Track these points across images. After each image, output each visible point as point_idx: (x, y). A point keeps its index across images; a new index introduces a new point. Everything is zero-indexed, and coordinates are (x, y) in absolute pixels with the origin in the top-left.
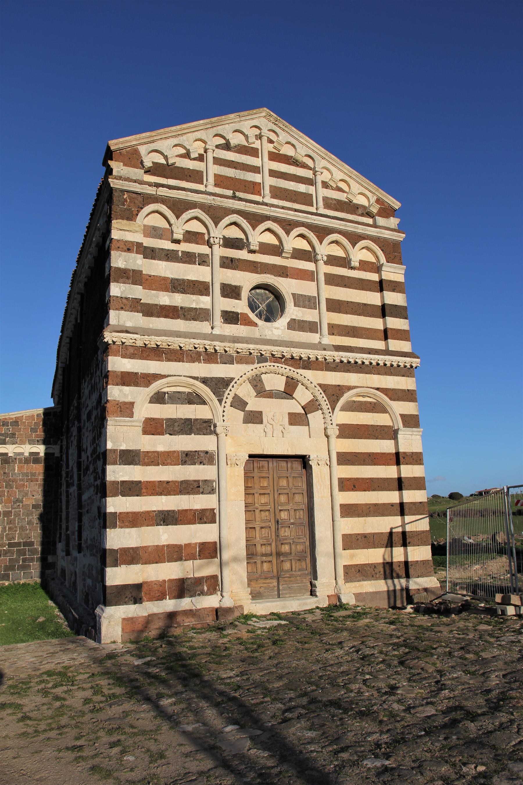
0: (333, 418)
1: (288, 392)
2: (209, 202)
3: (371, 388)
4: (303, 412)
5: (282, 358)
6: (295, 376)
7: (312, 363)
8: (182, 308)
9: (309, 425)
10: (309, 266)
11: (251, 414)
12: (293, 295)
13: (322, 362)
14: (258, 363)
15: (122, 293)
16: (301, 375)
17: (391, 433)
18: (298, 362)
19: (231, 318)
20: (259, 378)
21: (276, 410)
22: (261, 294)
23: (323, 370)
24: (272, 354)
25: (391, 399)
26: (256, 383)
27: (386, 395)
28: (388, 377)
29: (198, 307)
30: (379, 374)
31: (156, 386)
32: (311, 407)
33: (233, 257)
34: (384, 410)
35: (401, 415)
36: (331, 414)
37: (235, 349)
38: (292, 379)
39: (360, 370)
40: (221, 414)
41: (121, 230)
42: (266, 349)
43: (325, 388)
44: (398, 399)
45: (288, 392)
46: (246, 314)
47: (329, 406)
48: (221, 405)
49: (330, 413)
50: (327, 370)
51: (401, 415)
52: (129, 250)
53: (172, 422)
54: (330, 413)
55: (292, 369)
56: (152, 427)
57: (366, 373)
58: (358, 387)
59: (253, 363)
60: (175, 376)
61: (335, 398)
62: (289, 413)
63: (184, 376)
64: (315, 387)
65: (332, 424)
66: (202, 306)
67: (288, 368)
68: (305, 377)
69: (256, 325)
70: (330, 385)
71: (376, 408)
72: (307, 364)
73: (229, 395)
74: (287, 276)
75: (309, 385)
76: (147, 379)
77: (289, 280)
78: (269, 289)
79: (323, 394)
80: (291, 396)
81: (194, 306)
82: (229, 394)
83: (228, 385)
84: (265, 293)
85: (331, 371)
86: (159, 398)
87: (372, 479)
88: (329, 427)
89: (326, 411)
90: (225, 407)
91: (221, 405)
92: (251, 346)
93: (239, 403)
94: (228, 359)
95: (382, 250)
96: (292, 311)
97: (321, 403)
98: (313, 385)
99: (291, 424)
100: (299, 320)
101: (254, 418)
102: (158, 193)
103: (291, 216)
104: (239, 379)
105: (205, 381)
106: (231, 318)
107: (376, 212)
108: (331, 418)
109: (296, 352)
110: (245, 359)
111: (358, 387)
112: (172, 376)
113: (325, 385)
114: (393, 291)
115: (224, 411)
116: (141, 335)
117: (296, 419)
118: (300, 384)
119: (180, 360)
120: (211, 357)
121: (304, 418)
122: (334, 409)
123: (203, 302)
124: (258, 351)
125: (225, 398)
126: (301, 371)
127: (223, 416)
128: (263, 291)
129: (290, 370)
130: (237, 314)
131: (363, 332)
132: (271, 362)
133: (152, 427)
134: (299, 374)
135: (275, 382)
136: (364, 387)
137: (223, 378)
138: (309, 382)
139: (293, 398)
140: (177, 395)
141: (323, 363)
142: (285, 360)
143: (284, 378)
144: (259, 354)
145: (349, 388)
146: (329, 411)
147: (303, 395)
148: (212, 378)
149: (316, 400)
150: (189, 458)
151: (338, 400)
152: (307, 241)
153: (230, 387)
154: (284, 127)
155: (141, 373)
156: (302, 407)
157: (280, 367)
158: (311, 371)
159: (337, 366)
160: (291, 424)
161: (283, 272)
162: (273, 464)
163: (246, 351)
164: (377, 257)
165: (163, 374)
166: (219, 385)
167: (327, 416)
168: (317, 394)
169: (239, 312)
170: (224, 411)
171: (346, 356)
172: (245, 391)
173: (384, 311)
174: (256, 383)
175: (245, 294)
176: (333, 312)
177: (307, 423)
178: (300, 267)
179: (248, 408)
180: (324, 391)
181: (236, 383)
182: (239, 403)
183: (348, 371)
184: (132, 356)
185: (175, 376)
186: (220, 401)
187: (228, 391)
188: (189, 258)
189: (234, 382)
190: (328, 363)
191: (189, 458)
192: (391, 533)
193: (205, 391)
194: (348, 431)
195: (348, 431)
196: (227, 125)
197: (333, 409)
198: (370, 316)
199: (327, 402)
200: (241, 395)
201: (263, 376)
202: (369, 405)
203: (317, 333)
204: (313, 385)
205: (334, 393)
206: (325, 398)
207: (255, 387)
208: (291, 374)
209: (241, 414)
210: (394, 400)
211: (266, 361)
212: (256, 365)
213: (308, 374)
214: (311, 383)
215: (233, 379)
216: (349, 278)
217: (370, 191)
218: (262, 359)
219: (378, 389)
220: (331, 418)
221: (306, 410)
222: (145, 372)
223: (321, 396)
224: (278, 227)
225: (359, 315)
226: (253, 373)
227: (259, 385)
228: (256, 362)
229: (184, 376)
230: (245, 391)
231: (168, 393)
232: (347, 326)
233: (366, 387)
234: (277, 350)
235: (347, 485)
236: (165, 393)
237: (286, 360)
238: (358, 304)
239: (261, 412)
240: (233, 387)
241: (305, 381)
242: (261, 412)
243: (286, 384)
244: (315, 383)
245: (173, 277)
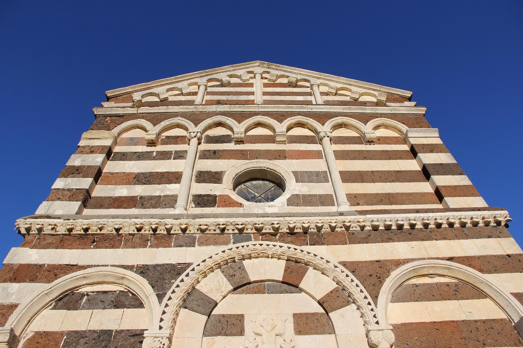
0: (379, 311)
1: (291, 283)
2: (191, 111)
3: (438, 258)
4: (323, 311)
5: (274, 235)
6: (299, 255)
7: (324, 236)
8: (141, 198)
9: (334, 332)
11: (223, 320)
12: (293, 172)
13: (342, 233)
14: (234, 243)
15: (65, 185)
16: (309, 253)
18: (303, 238)
20: (239, 266)
22: (260, 186)
23: (346, 244)
24: (257, 229)
25: (481, 271)
27: (470, 266)
28: (462, 241)
29: (162, 195)
30: (445, 239)
33: (216, 149)
34: (478, 293)
36: (373, 306)
37: (197, 227)
38: (297, 262)
39: (410, 236)
40: (159, 316)
41: (90, 139)
43: (353, 267)
45: (291, 283)
46: (228, 196)
47: (366, 293)
48: (160, 302)
49: (369, 304)
50: (352, 242)
52: (92, 152)
54: (369, 304)
55: (293, 246)
57: (423, 240)
58: (413, 260)
60: (98, 266)
61: (374, 280)
62: (295, 315)
63: (112, 266)
64: (336, 267)
65: (377, 323)
66: (168, 193)
67: (285, 246)
68: (315, 255)
70: (362, 262)
73: (179, 288)
74: (285, 158)
75: (325, 266)
77: (287, 161)
78: (268, 178)
79: (351, 276)
80: (297, 287)
82: (178, 286)
83: (179, 274)
84: (265, 184)
85: (359, 243)
86: (68, 301)
88: (372, 326)
89: (363, 303)
90: (167, 305)
91: (160, 302)
93: (195, 301)
95: (403, 123)
97: (351, 290)
98: (331, 265)
99: (299, 332)
100: (304, 196)
102: (139, 112)
103: (283, 108)
104: (199, 265)
107: (385, 100)
108: (373, 313)
111: (413, 260)
112: (95, 266)
113: (352, 263)
115: (164, 313)
116: (65, 220)
118: (311, 269)
121: (324, 321)
122: (377, 297)
123: (170, 190)
124: (234, 228)
125: (171, 290)
126: (307, 248)
127: (162, 320)
128: (261, 182)
129: (289, 248)
130: (215, 196)
131: (404, 198)
132: (256, 239)
134: (305, 252)
136: (424, 259)
137: (173, 265)
138: (324, 261)
139: (301, 290)
140: (102, 297)
141: (344, 234)
142: (281, 236)
144: (236, 231)
145: (398, 263)
146: (367, 301)
148: (156, 266)
149: (343, 289)
151: (381, 283)
152: (309, 129)
153: (183, 276)
154: (277, 68)
155: (49, 265)
156: (319, 302)
157: (271, 246)
158: (325, 246)
159: (370, 236)
160: (299, 332)
163: (214, 228)
164: (400, 131)
165: (81, 263)
167: (367, 309)
168: (342, 277)
169: (217, 194)
170: (164, 313)
171: (381, 220)
172: (216, 285)
173: (426, 173)
176: (352, 182)
177: (332, 331)
178: (301, 149)
180: (353, 272)
181: (193, 270)
182: (195, 301)
185: (98, 266)
186: (160, 297)
187: (177, 282)
188: (164, 156)
189: (191, 268)
190: (353, 234)
193: (142, 287)
196: (222, 73)
197: (375, 298)
198: (410, 181)
199: (362, 287)
201: (246, 263)
202: (446, 289)
203: (334, 205)
204: (331, 265)
206: (356, 281)
207: (230, 277)
208: (291, 253)
209: (200, 320)
211: (249, 239)
213: (321, 251)
214: (328, 262)
215: (189, 265)
216: (368, 151)
217: (374, 90)
219: (450, 259)
220: (373, 313)
221: (324, 305)
222: (54, 263)
223: (349, 279)
224: (269, 118)
225: (393, 181)
226: (225, 256)
227: (238, 274)
228: (232, 241)
229: (112, 266)
230: (216, 285)
231: (88, 295)
232: (377, 194)
233: (428, 259)
236: (83, 295)
237: (283, 235)
238: (389, 172)
239: (242, 316)
240: (187, 275)
241: (316, 261)
242: (242, 316)
243: (285, 270)
244: (334, 261)
245: (138, 172)
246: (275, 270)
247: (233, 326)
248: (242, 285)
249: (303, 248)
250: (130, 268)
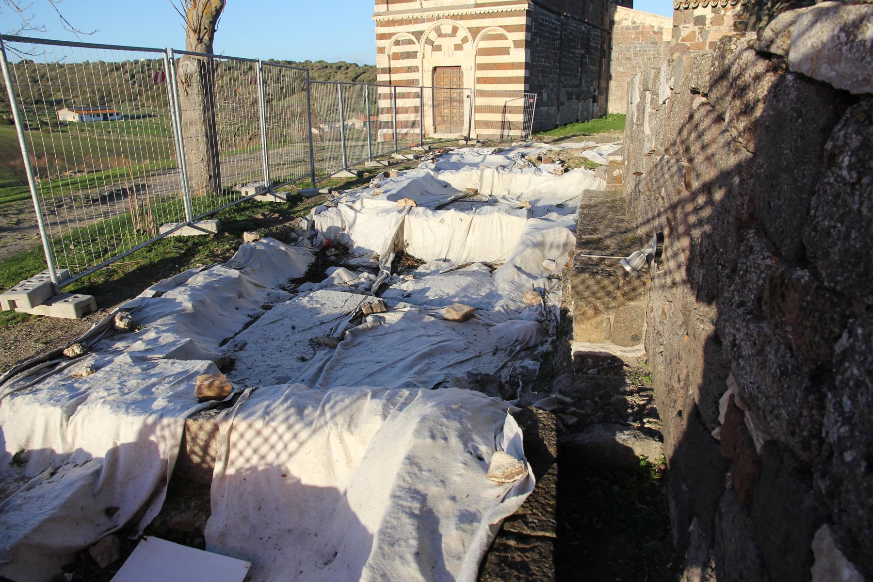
17: (505, 51)
21: (447, 43)
26: (438, 31)
31: (394, 38)
32: (465, 40)
34: (506, 38)
35: (514, 41)
42: (441, 13)
43: (470, 29)
44: (513, 31)
51: (514, 41)
53: (402, 53)
56: (396, 56)
71: (502, 37)
72: (462, 17)
73: (423, 38)
86: (397, 43)
87: (496, 78)
92: (431, 13)
94: (423, 21)
101: (438, 48)
105: (413, 33)
109: (456, 12)
117: (458, 47)
119: (402, 24)
120: (416, 21)
133: (396, 56)
135: (447, 28)
143: (451, 27)
145: (484, 28)
150: (410, 69)
162: (446, 69)
166: (418, 34)
172: (433, 36)
174: (438, 31)
182: (429, 42)
183: (483, 18)
184: (384, 26)
191: (410, 69)
192: (505, 106)
193: (413, 38)
194: (482, 52)
195: (482, 52)
205: (474, 32)
207: (437, 33)
218: (438, 18)
230: (433, 36)
234: (446, 13)
235: (480, 80)
246: (450, 31)
247: (438, 48)
248: (440, 35)
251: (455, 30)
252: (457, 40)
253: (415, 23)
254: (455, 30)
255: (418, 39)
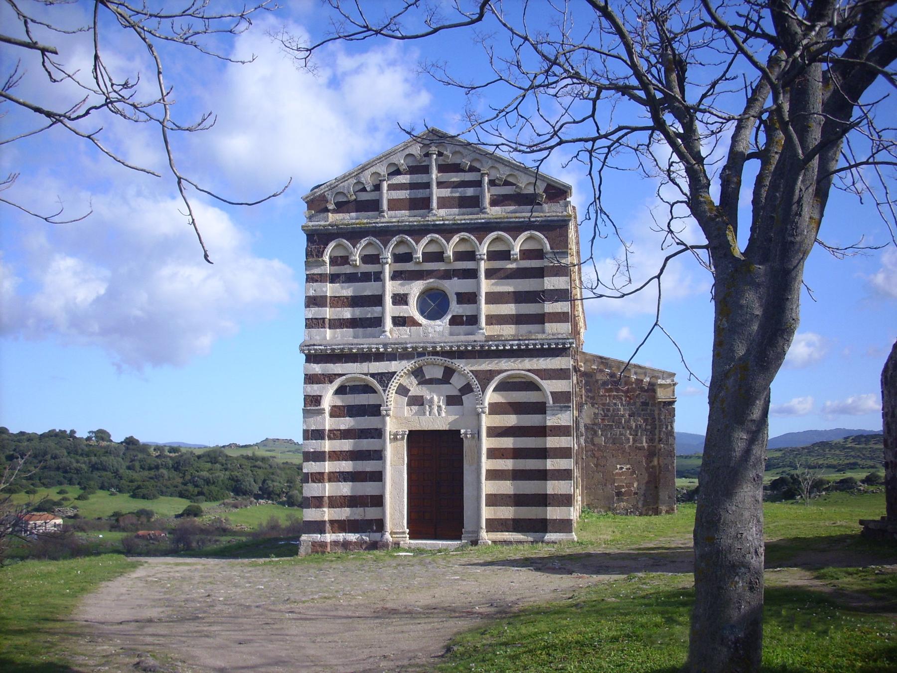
10: (469, 265)
19: (399, 321)
32: (467, 389)
35: (551, 393)
51: (551, 393)
59: (413, 358)
66: (376, 315)
69: (420, 325)
73: (394, 385)
76: (331, 378)
81: (369, 316)
94: (392, 357)
96: (456, 308)
105: (373, 375)
106: (399, 321)
110: (405, 355)
114: (555, 275)
120: (379, 357)
143: (443, 369)
145: (500, 372)
147: (457, 382)
161: (447, 275)
166: (385, 378)
174: (417, 373)
175: (413, 301)
179: (410, 394)
193: (374, 382)
200: (404, 384)
210: (545, 379)
212: (416, 360)
215: (395, 373)
246: (439, 373)
249: (453, 361)
250: (366, 374)
251: (449, 373)
252: (453, 389)
253: (376, 360)
254: (449, 373)
255: (385, 386)
